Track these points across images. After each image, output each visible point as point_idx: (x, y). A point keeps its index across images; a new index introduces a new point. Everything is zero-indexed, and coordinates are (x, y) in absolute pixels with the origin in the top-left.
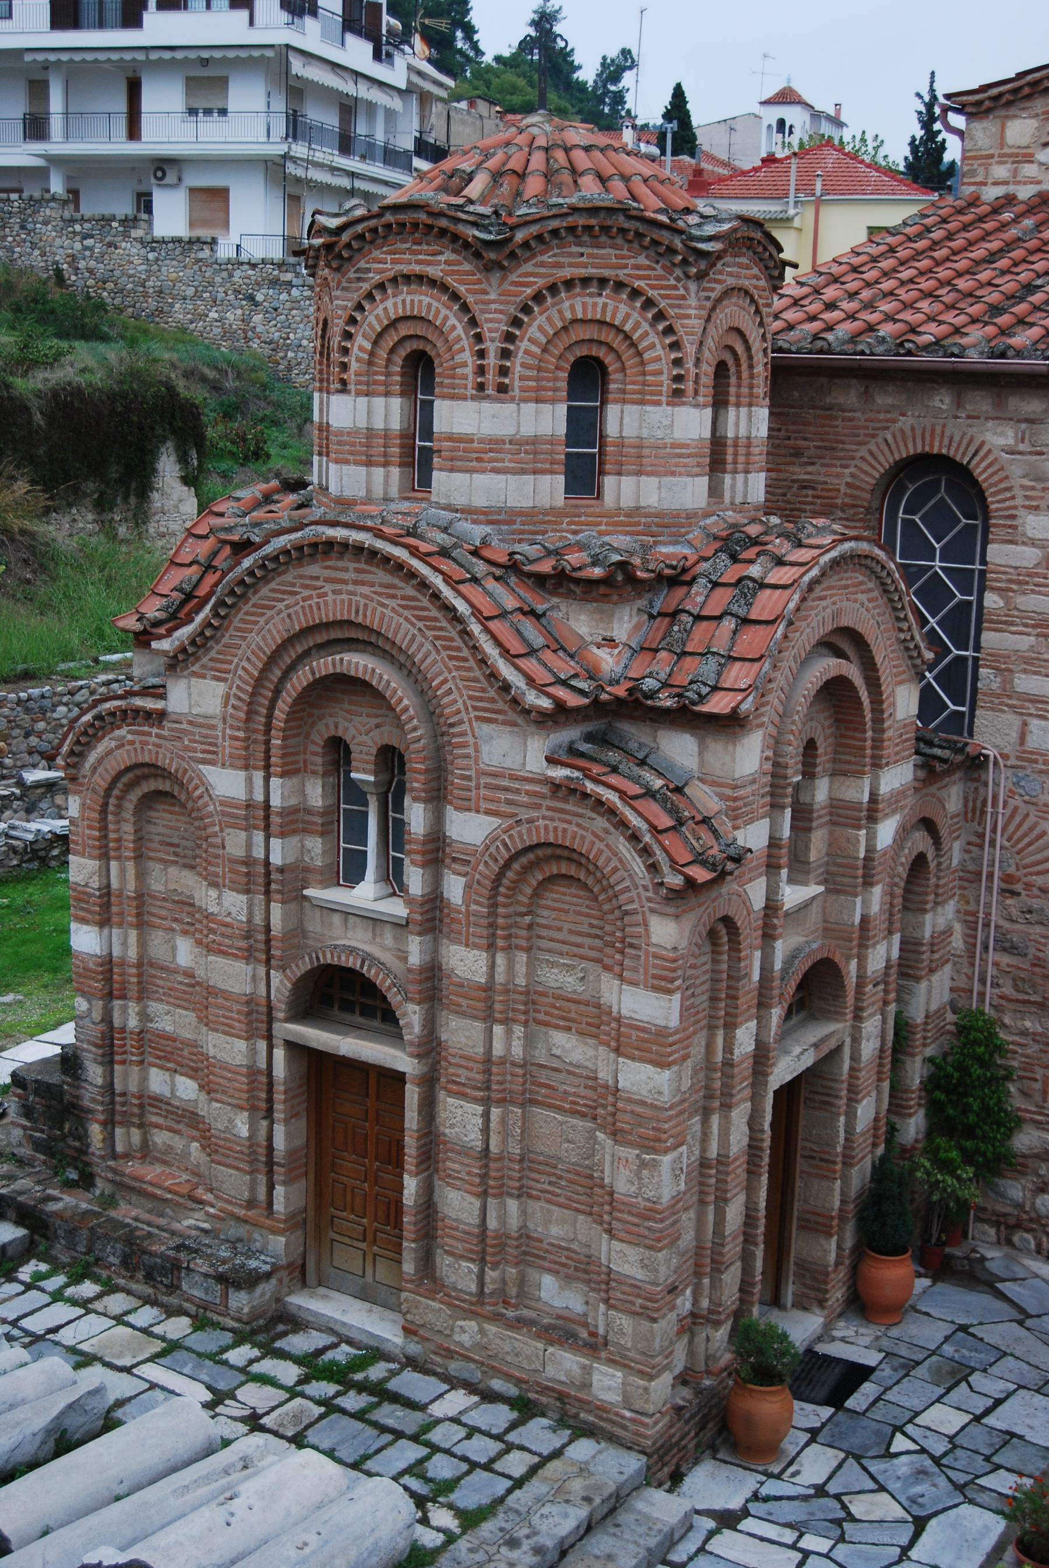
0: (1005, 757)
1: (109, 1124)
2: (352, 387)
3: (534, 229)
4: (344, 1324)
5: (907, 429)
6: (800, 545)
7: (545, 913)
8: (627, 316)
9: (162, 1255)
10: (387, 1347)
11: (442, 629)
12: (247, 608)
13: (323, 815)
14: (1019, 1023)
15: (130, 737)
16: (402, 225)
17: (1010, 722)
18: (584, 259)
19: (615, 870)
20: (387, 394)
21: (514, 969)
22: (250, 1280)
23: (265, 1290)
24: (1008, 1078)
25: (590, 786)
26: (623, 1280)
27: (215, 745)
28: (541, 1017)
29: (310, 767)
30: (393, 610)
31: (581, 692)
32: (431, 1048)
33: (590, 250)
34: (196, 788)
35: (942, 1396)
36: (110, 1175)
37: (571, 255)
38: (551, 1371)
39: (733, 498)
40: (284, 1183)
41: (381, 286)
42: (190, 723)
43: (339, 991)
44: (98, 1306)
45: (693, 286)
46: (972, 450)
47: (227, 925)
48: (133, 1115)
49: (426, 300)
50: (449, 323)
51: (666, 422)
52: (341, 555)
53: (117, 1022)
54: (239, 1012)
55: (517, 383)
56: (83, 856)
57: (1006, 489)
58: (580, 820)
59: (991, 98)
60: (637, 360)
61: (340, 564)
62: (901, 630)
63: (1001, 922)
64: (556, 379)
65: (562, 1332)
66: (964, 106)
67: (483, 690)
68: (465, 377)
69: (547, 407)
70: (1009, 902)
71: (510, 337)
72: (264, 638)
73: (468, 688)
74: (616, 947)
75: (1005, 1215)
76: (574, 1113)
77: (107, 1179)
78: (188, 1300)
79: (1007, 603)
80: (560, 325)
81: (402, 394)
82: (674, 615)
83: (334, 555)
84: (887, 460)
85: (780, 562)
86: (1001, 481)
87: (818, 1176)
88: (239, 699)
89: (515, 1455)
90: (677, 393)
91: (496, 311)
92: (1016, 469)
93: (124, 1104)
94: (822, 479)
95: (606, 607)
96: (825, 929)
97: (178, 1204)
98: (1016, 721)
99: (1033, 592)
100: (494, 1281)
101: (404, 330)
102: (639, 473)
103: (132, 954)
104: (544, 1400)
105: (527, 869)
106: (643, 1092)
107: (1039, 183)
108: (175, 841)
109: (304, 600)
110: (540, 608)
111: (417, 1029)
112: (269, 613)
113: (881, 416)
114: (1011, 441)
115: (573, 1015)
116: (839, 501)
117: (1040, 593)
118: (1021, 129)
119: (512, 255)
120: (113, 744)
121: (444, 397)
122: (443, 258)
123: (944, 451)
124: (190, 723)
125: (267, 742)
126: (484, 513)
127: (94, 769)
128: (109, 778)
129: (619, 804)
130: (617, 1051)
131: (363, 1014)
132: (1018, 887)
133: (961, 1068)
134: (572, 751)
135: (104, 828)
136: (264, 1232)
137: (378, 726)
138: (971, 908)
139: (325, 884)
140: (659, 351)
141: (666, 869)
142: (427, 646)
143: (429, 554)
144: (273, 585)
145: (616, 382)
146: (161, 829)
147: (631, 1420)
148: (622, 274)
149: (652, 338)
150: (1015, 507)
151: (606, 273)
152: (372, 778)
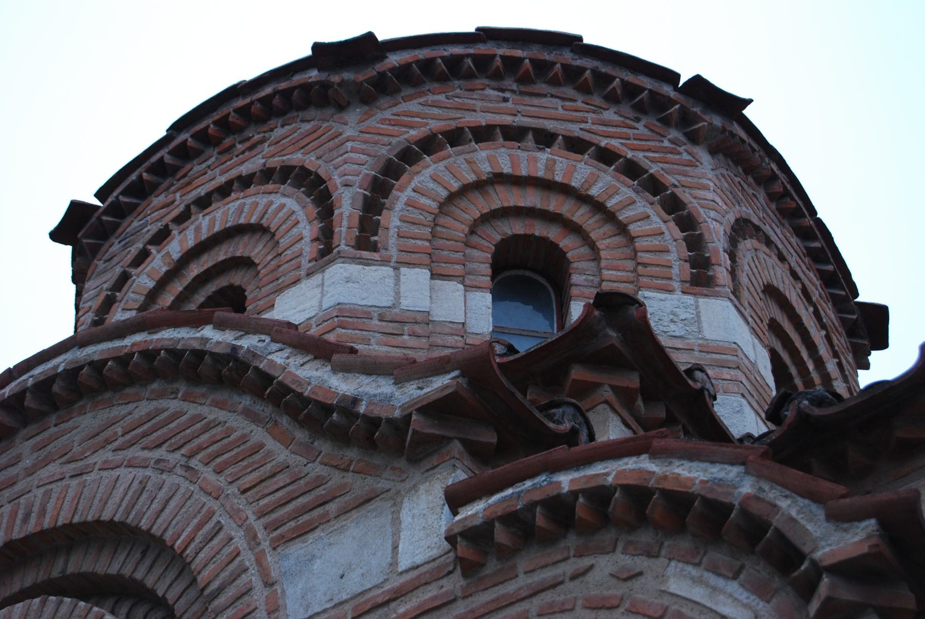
18: (509, 105)
30: (107, 467)
60: (618, 239)
80: (471, 178)
145: (582, 272)
148: (575, 130)
151: (550, 125)
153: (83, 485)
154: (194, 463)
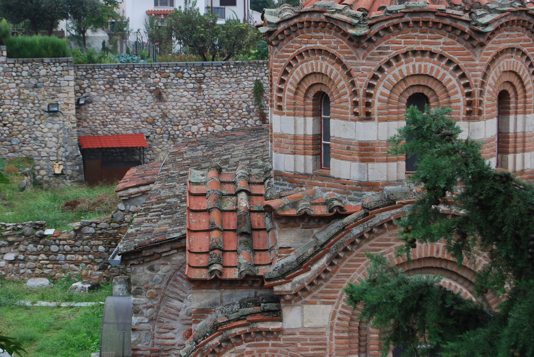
2: (376, 117)
15: (248, 349)
16: (416, 23)
20: (398, 119)
27: (325, 344)
37: (504, 36)
41: (397, 58)
42: (303, 333)
49: (430, 65)
68: (458, 108)
71: (483, 84)
88: (345, 313)
122: (441, 41)
124: (303, 333)
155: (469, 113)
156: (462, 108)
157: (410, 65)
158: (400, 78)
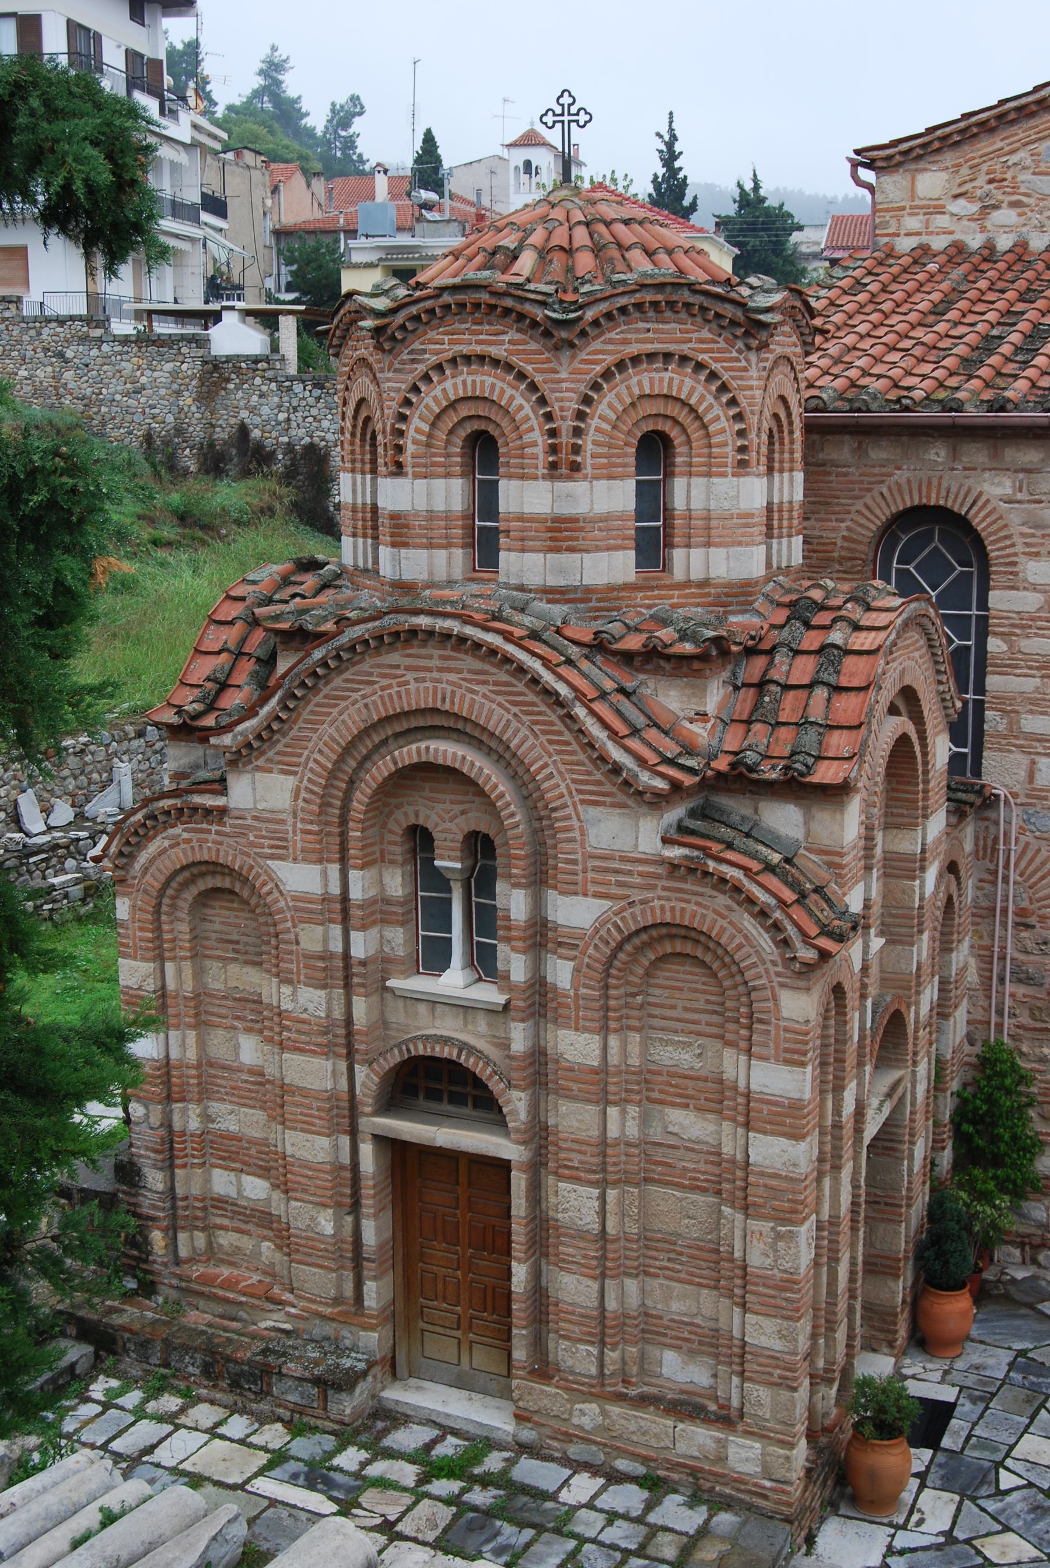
0: (1015, 795)
1: (172, 1231)
2: (409, 470)
3: (603, 307)
4: (448, 1415)
5: (903, 481)
6: (869, 608)
7: (657, 992)
8: (692, 390)
9: (249, 1362)
10: (497, 1435)
11: (540, 713)
12: (316, 700)
13: (402, 904)
14: (1037, 1050)
15: (185, 835)
16: (462, 305)
17: (1018, 762)
18: (650, 335)
19: (740, 946)
20: (447, 475)
21: (627, 1050)
22: (347, 1382)
23: (362, 1389)
24: (1029, 1105)
25: (712, 865)
26: (761, 1352)
28: (655, 1095)
29: (387, 857)
30: (484, 696)
31: (690, 770)
32: (540, 1134)
33: (656, 326)
34: (264, 884)
35: (1028, 1426)
36: (174, 1282)
37: (637, 331)
38: (682, 1447)
39: (779, 562)
40: (375, 1278)
41: (439, 368)
43: (431, 1080)
44: (182, 1420)
45: (753, 357)
46: (970, 500)
47: (303, 1021)
48: (196, 1218)
49: (489, 380)
50: (516, 403)
51: (733, 493)
52: (424, 644)
53: (177, 1126)
54: (319, 1109)
55: (589, 461)
56: (135, 959)
57: (1006, 537)
58: (700, 899)
59: (901, 153)
61: (423, 651)
62: (940, 682)
63: (1017, 955)
64: (625, 455)
65: (686, 1408)
66: (873, 160)
67: (589, 773)
69: (617, 483)
70: (1024, 934)
71: (581, 416)
72: (337, 729)
73: (573, 772)
74: (742, 1021)
75: (1029, 1236)
76: (693, 1188)
77: (171, 1286)
78: (280, 1406)
79: (1010, 647)
80: (628, 401)
81: (463, 475)
82: (761, 685)
83: (415, 643)
84: (884, 514)
85: (857, 627)
86: (1000, 529)
87: (883, 1220)
89: (663, 1538)
90: (742, 464)
91: (568, 390)
92: (1015, 519)
93: (186, 1208)
94: (817, 533)
95: (698, 681)
96: (883, 979)
97: (253, 1307)
98: (1025, 760)
99: (1037, 635)
100: (614, 1362)
101: (464, 411)
102: (708, 545)
103: (192, 1055)
104: (675, 1476)
105: (640, 950)
106: (777, 1165)
107: (951, 233)
108: (235, 937)
109: (383, 689)
110: (629, 685)
111: (523, 1116)
112: (343, 704)
113: (876, 471)
114: (1009, 491)
115: (691, 1092)
116: (836, 555)
117: (1043, 636)
118: (932, 182)
119: (583, 334)
120: (167, 843)
121: (510, 477)
122: (506, 338)
123: (942, 502)
125: (343, 836)
126: (562, 593)
127: (145, 870)
128: (162, 878)
129: (746, 881)
130: (747, 1126)
131: (451, 1102)
132: (1033, 920)
133: (989, 1100)
134: (681, 828)
135: (158, 929)
136: (354, 1329)
137: (463, 813)
138: (986, 942)
139: (406, 974)
140: (723, 423)
141: (798, 944)
142: (524, 731)
143: (521, 638)
144: (347, 675)
145: (681, 455)
146: (217, 927)
147: (771, 1489)
148: (685, 349)
149: (717, 410)
150: (1015, 554)
151: (671, 348)
152: (459, 865)
153: (473, 700)
154: (536, 728)
155: (553, 466)
156: (541, 456)
157: (459, 380)
158: (445, 403)
